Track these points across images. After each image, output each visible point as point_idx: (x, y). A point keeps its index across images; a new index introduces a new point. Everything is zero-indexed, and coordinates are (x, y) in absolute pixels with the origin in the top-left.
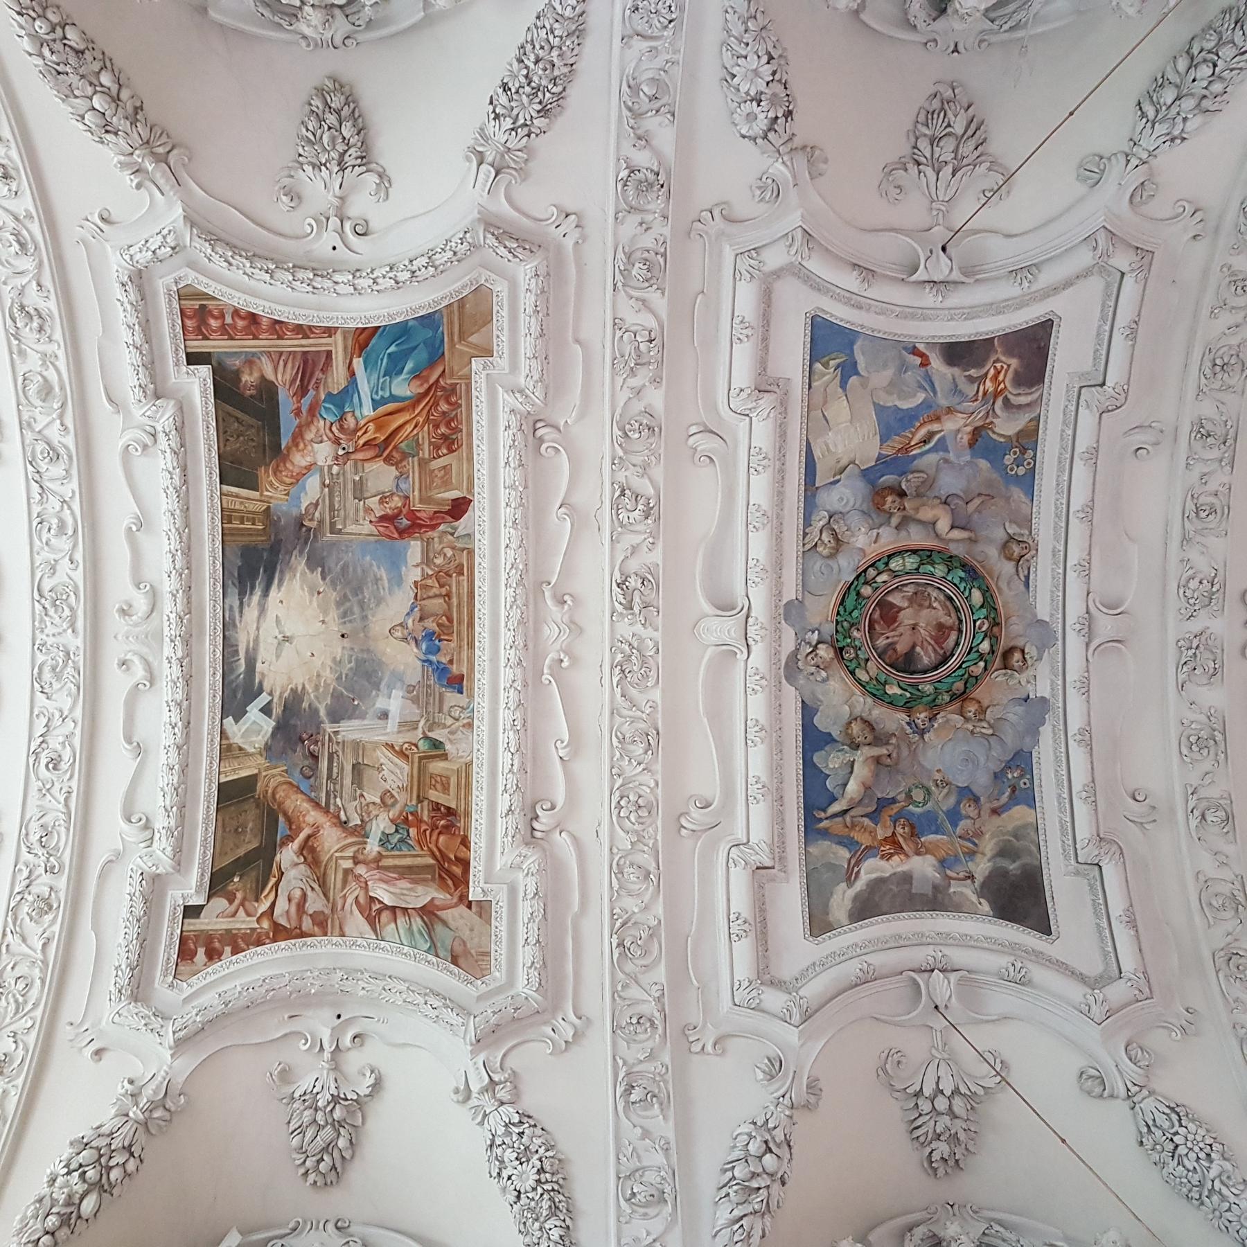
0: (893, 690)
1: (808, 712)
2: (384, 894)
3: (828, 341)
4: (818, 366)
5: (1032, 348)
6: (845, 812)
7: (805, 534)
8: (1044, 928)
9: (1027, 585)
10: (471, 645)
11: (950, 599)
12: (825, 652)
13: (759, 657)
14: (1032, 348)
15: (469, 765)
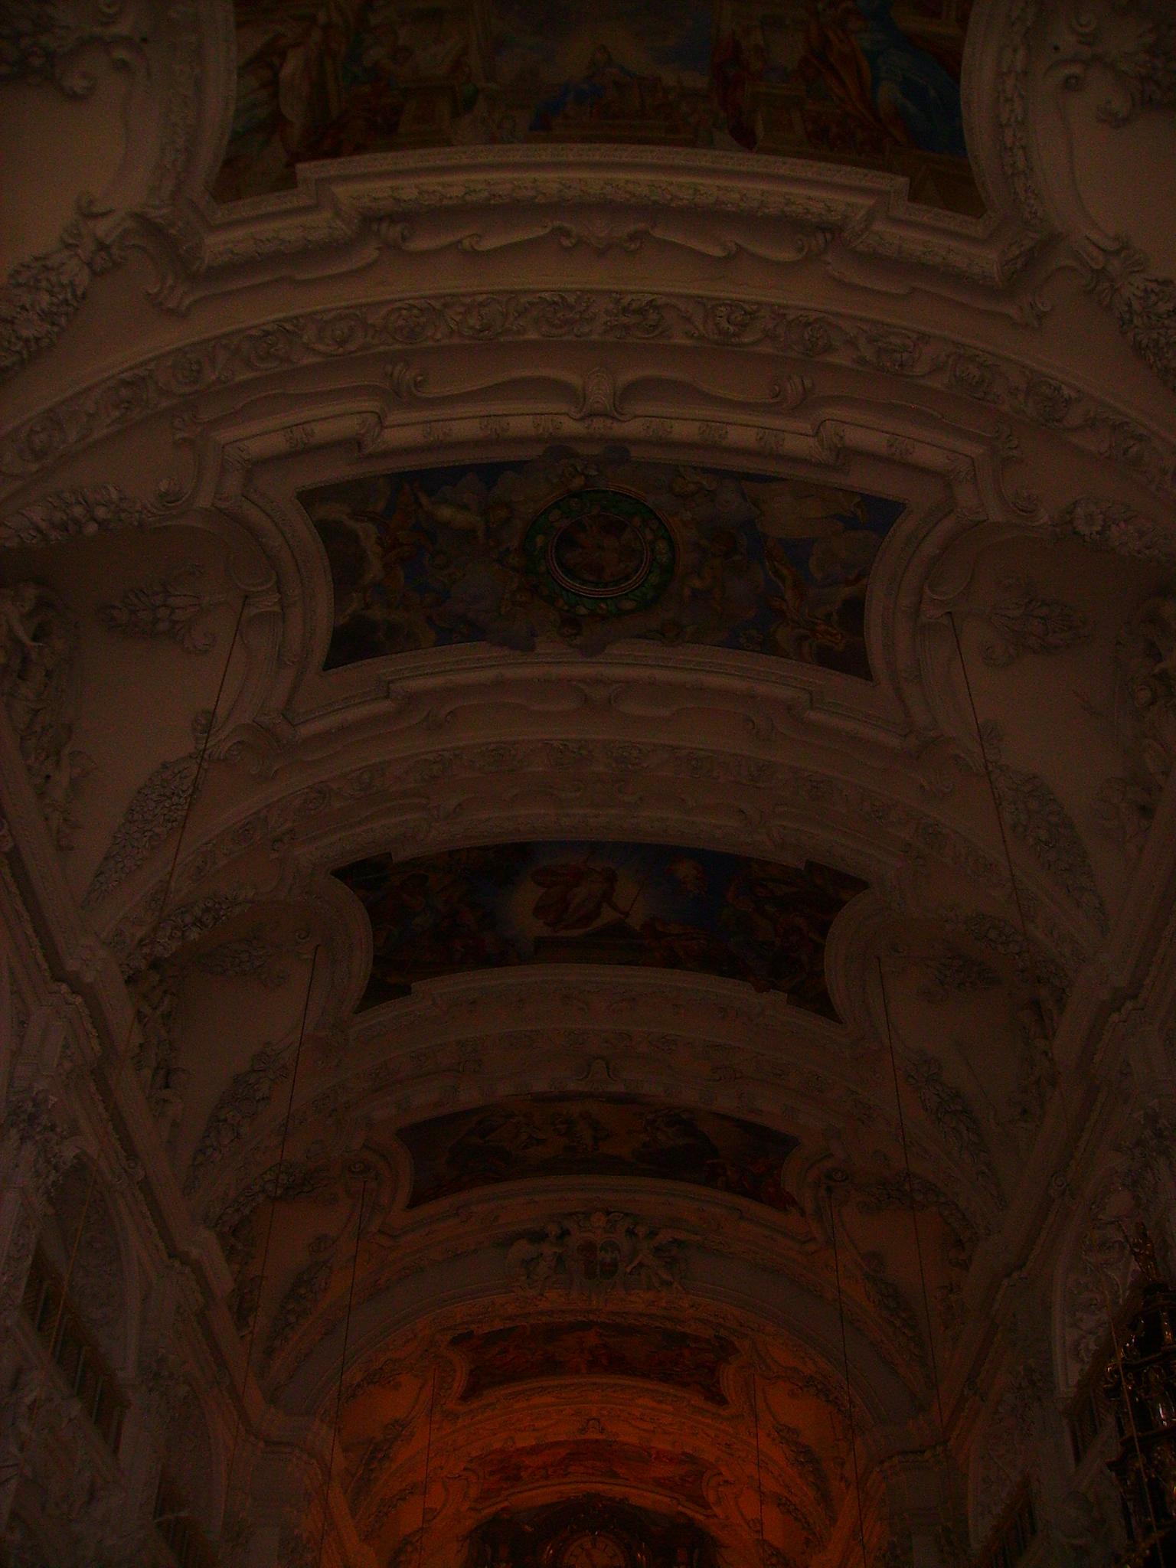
0: (540, 540)
1: (518, 466)
2: (291, 67)
3: (878, 515)
4: (857, 499)
5: (852, 661)
6: (421, 505)
7: (695, 468)
8: (330, 664)
9: (639, 637)
10: (584, 140)
11: (627, 578)
12: (578, 482)
13: (571, 426)
14: (852, 661)
15: (450, 144)
